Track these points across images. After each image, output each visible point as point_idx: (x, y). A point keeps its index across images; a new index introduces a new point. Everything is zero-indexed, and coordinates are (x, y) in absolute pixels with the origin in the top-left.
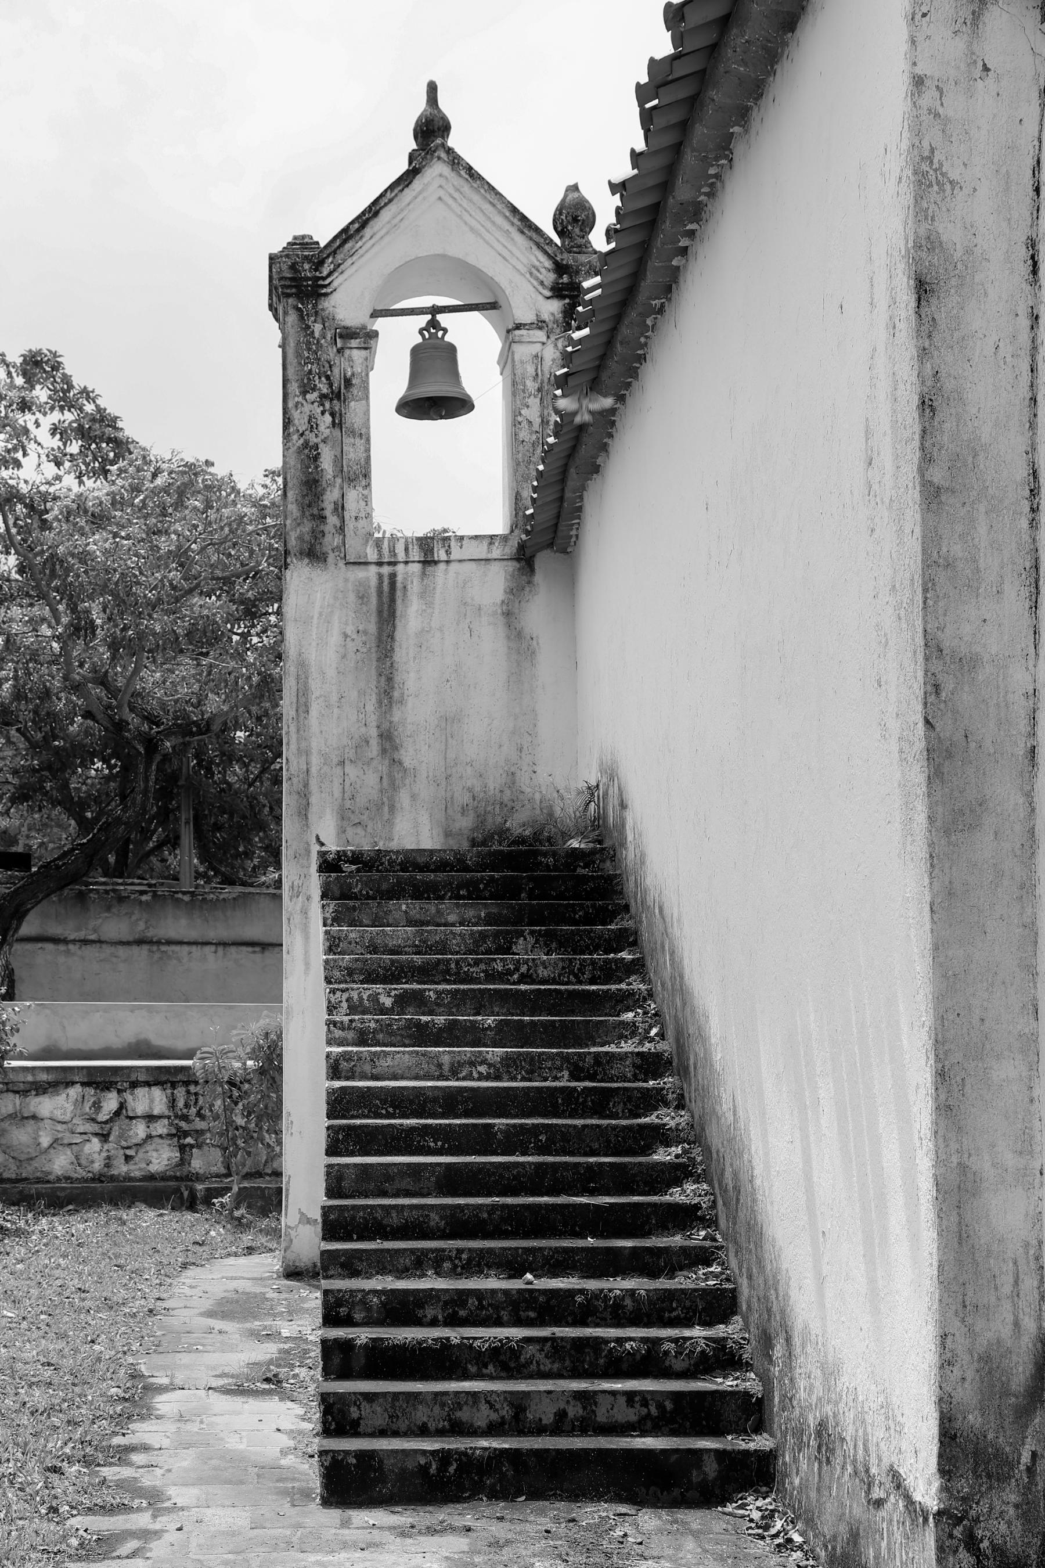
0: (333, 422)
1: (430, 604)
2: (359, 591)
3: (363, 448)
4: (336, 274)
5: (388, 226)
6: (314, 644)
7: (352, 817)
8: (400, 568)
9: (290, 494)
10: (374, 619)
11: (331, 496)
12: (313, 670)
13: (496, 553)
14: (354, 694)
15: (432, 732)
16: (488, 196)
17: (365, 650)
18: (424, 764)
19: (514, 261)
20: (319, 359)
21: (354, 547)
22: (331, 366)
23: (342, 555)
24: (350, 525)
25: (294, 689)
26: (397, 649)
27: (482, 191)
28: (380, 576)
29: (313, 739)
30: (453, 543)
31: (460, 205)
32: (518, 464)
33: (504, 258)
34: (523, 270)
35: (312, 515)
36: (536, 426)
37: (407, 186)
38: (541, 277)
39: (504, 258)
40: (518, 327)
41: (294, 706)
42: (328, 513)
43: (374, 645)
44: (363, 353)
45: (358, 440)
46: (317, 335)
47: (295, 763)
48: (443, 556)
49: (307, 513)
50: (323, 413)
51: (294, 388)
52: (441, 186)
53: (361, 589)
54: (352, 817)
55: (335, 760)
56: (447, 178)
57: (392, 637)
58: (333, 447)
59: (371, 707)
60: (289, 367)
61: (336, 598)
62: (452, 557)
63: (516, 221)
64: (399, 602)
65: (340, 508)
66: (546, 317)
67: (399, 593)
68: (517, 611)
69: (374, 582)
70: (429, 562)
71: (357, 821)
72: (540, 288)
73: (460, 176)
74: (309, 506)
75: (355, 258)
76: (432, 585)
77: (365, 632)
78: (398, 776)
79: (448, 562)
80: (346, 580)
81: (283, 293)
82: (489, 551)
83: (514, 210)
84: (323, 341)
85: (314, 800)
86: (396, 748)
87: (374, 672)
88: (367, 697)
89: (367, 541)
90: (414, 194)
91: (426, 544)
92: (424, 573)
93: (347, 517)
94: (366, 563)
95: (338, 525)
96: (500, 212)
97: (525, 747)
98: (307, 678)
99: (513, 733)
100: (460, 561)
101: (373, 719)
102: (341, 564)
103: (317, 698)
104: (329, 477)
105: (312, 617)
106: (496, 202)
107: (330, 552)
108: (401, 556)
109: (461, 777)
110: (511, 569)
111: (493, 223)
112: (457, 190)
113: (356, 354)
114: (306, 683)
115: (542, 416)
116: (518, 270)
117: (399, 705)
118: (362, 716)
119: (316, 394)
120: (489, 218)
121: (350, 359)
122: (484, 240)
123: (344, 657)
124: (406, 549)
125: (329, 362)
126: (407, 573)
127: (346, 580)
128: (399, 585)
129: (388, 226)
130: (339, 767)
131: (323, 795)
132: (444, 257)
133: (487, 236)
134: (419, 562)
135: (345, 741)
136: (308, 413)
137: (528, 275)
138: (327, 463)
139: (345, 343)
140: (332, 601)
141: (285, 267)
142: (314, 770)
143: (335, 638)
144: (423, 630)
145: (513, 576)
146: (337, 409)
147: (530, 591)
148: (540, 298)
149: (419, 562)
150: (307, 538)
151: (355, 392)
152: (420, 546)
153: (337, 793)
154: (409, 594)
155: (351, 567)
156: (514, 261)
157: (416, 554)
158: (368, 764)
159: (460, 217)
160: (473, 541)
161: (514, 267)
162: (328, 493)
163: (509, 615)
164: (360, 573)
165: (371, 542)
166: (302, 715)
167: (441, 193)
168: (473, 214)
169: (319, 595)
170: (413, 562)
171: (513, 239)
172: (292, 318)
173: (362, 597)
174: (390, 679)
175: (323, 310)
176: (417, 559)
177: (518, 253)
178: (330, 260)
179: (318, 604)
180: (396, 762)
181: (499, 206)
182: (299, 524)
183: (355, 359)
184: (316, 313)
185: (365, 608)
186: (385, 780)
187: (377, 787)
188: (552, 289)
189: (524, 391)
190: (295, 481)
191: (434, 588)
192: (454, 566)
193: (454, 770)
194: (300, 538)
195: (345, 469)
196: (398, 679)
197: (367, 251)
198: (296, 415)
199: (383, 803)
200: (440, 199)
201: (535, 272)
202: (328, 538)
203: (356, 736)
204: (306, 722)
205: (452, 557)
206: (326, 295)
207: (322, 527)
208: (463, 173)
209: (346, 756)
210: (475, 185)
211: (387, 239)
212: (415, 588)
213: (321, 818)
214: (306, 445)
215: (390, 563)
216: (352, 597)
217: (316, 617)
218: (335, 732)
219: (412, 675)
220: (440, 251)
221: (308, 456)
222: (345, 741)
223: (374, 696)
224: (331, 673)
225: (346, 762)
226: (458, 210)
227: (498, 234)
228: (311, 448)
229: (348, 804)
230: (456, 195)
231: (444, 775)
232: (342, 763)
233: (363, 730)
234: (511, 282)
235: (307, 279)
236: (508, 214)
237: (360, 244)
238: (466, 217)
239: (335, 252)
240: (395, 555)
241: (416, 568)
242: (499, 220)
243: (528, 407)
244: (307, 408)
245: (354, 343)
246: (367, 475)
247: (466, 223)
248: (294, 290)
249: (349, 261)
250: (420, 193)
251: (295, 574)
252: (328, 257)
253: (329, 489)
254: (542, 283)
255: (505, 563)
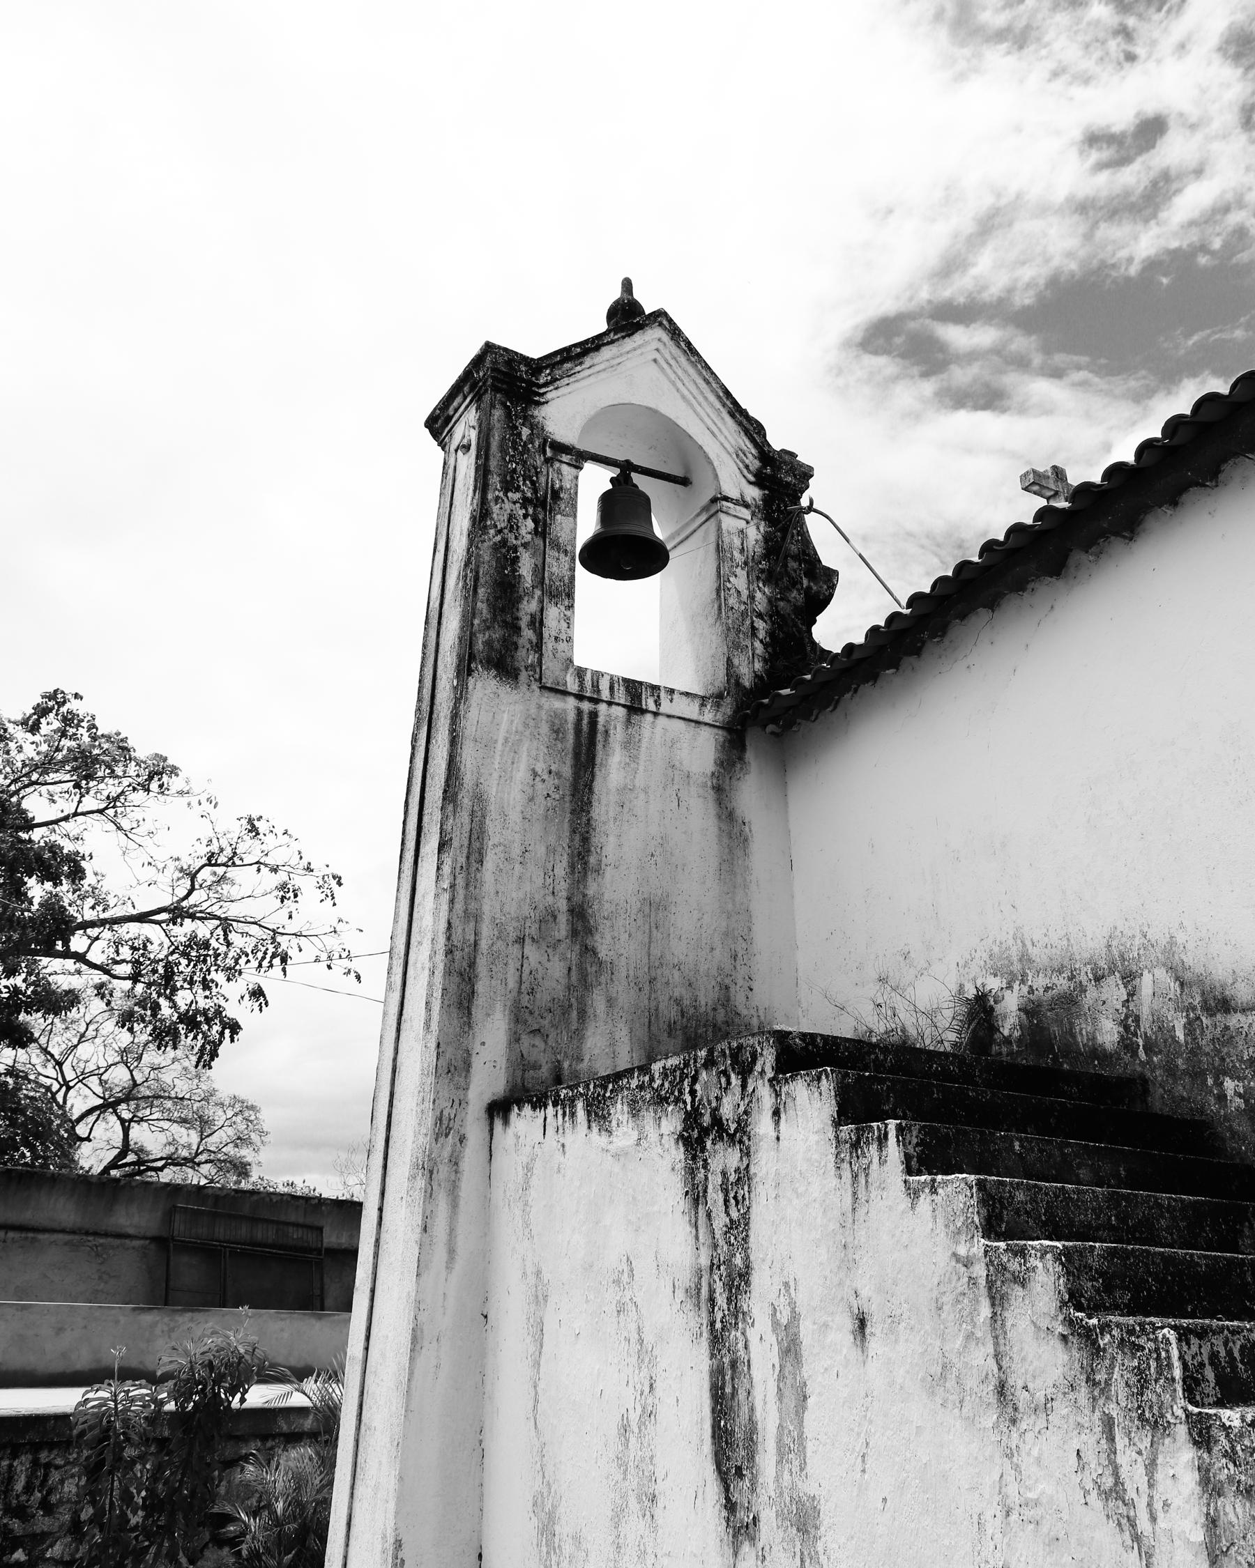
0: (536, 529)
1: (634, 758)
2: (553, 724)
3: (567, 566)
4: (551, 388)
5: (607, 364)
6: (496, 775)
7: (530, 1019)
8: (602, 708)
9: (481, 591)
10: (569, 761)
11: (529, 607)
12: (493, 808)
13: (708, 717)
14: (541, 850)
15: (633, 917)
16: (704, 373)
17: (557, 797)
18: (623, 958)
19: (722, 439)
20: (525, 462)
21: (551, 668)
22: (537, 473)
23: (537, 676)
24: (549, 645)
25: (467, 828)
26: (595, 804)
27: (699, 366)
28: (579, 712)
29: (486, 900)
30: (663, 694)
31: (675, 372)
32: (729, 629)
33: (712, 433)
34: (731, 450)
35: (504, 621)
36: (744, 597)
37: (629, 335)
38: (747, 461)
39: (712, 433)
40: (726, 499)
41: (465, 851)
42: (523, 623)
43: (568, 793)
44: (573, 471)
45: (562, 556)
46: (524, 438)
47: (460, 931)
48: (652, 707)
49: (499, 618)
50: (525, 516)
51: (495, 480)
52: (657, 350)
53: (556, 721)
54: (530, 1019)
55: (513, 935)
56: (665, 344)
57: (589, 787)
58: (533, 555)
59: (561, 870)
60: (491, 458)
61: (526, 725)
62: (662, 710)
63: (728, 403)
64: (599, 747)
65: (537, 623)
66: (748, 499)
67: (600, 737)
68: (727, 788)
69: (571, 717)
70: (635, 709)
71: (536, 1027)
72: (745, 472)
73: (679, 346)
74: (503, 610)
75: (572, 379)
76: (637, 736)
77: (559, 775)
78: (592, 970)
79: (656, 714)
80: (540, 707)
81: (493, 385)
82: (701, 713)
83: (728, 394)
84: (530, 446)
85: (480, 987)
86: (589, 931)
87: (566, 826)
88: (557, 858)
89: (567, 668)
90: (635, 345)
91: (633, 688)
92: (628, 722)
93: (546, 635)
94: (565, 693)
95: (534, 640)
96: (713, 391)
97: (740, 955)
98: (484, 817)
99: (726, 934)
100: (669, 716)
101: (563, 887)
102: (535, 686)
103: (494, 845)
104: (527, 585)
105: (496, 742)
106: (711, 380)
107: (522, 668)
108: (605, 694)
109: (667, 983)
110: (722, 739)
111: (706, 398)
112: (675, 359)
113: (565, 468)
114: (482, 824)
115: (748, 588)
116: (725, 448)
117: (594, 875)
118: (549, 881)
119: (517, 496)
120: (702, 393)
121: (559, 472)
122: (695, 411)
123: (531, 799)
124: (612, 688)
125: (536, 468)
126: (609, 716)
127: (540, 707)
128: (600, 727)
129: (607, 364)
130: (517, 946)
131: (493, 982)
132: (654, 412)
133: (699, 409)
134: (624, 706)
135: (526, 910)
136: (509, 511)
137: (734, 456)
138: (526, 568)
139: (555, 454)
140: (521, 728)
141: (500, 360)
142: (484, 945)
143: (521, 775)
144: (625, 788)
145: (723, 746)
146: (541, 517)
147: (742, 769)
148: (744, 481)
149: (624, 706)
150: (497, 645)
151: (563, 506)
152: (627, 689)
153: (512, 984)
154: (611, 740)
155: (546, 694)
156: (722, 439)
157: (621, 696)
158: (555, 949)
159: (673, 383)
160: (684, 698)
161: (722, 444)
162: (525, 603)
163: (721, 790)
164: (557, 703)
165: (571, 670)
166: (475, 865)
167: (657, 356)
168: (687, 384)
169: (505, 716)
170: (618, 704)
171: (723, 419)
172: (498, 413)
173: (557, 731)
174: (585, 840)
175: (532, 416)
176: (622, 701)
177: (727, 433)
178: (548, 371)
179: (504, 727)
180: (588, 951)
181: (714, 385)
182: (488, 628)
183: (565, 473)
184: (525, 418)
185: (559, 745)
186: (574, 973)
187: (564, 981)
188: (755, 476)
189: (731, 559)
190: (488, 578)
191: (640, 740)
192: (662, 721)
193: (659, 972)
194: (488, 643)
195: (547, 581)
196: (595, 840)
197: (583, 379)
198: (495, 509)
199: (570, 1006)
200: (655, 361)
201: (742, 455)
202: (521, 653)
203: (541, 907)
204: (478, 875)
205: (662, 710)
206: (539, 404)
207: (515, 638)
208: (682, 344)
209: (527, 931)
210: (693, 359)
211: (603, 375)
212: (618, 736)
213: (488, 1015)
214: (504, 542)
215: (591, 700)
216: (545, 729)
217: (501, 741)
218: (514, 895)
219: (612, 839)
220: (653, 406)
221: (505, 557)
222: (526, 910)
223: (565, 856)
224: (515, 817)
225: (527, 938)
226: (673, 376)
227: (709, 410)
228: (510, 548)
229: (525, 1000)
230: (672, 362)
231: (647, 978)
232: (521, 941)
233: (550, 899)
234: (718, 456)
235: (523, 380)
236: (721, 394)
237: (578, 368)
238: (680, 385)
239: (553, 366)
240: (599, 691)
241: (620, 712)
242: (712, 398)
243: (736, 576)
244: (508, 506)
245: (565, 458)
246: (570, 595)
247: (678, 390)
248: (504, 386)
249: (566, 381)
250: (640, 347)
251: (479, 684)
252: (546, 368)
253: (526, 598)
254: (747, 467)
255: (716, 731)
